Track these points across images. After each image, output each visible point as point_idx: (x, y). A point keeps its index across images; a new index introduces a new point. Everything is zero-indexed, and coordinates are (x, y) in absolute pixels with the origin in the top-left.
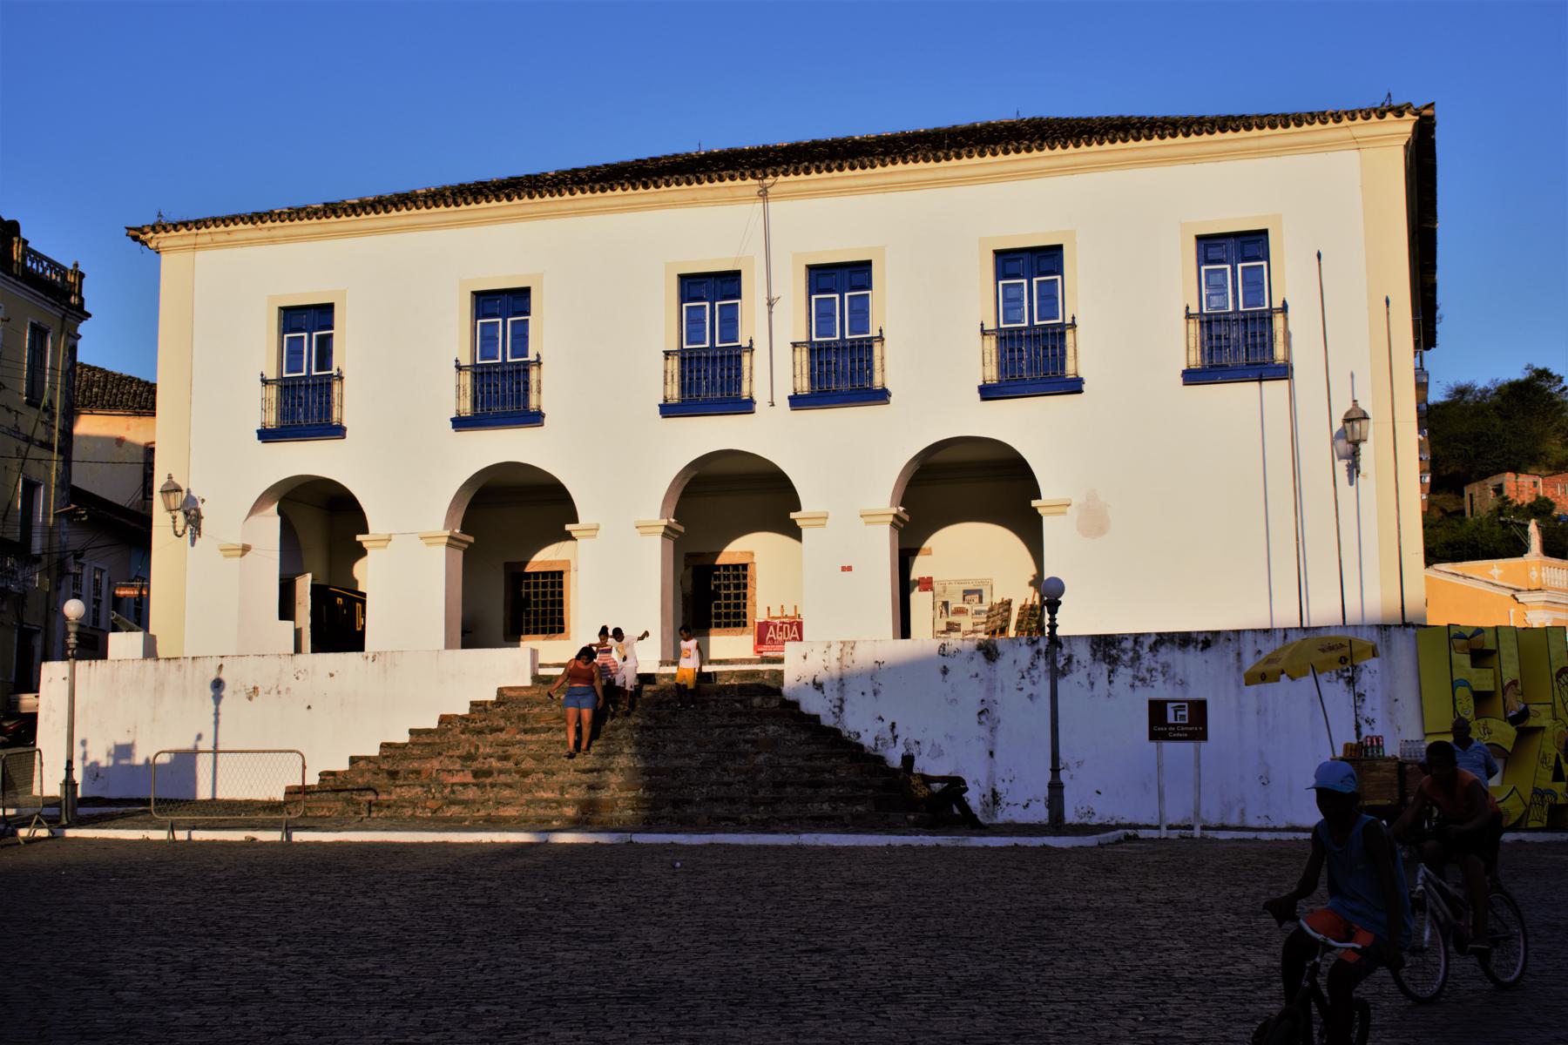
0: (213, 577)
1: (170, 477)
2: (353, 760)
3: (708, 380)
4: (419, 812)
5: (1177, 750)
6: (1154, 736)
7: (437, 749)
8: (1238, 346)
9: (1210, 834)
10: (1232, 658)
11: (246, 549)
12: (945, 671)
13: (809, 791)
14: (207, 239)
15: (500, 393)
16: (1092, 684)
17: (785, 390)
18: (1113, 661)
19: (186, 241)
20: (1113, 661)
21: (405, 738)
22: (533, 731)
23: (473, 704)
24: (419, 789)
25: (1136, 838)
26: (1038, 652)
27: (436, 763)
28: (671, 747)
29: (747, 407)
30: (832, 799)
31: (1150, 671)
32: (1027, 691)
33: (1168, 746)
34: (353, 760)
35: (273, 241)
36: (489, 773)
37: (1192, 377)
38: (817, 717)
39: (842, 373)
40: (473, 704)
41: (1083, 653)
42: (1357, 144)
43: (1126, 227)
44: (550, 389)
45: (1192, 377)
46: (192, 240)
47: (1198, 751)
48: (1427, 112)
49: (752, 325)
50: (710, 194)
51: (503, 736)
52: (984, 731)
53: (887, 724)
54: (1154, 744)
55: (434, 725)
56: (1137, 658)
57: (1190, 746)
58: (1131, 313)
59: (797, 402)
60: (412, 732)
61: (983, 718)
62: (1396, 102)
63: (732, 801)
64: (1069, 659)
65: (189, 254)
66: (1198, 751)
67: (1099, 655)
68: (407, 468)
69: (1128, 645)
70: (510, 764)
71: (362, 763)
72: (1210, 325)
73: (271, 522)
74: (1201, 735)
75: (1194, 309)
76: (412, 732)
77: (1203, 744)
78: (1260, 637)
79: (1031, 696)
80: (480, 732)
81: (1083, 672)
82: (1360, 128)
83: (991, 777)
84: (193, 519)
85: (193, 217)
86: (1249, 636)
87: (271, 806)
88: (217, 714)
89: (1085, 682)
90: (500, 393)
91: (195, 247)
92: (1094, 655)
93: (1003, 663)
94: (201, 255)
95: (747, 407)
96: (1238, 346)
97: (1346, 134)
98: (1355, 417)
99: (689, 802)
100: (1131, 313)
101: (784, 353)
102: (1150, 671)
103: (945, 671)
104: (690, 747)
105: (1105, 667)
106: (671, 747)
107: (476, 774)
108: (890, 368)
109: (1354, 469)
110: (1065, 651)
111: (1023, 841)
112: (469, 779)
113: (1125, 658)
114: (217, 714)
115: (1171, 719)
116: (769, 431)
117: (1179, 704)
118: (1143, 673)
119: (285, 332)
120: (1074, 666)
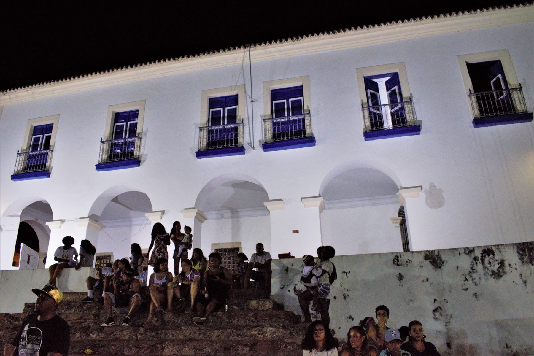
12: (401, 277)
16: (525, 282)
26: (476, 259)
32: (471, 291)
37: (478, 122)
38: (361, 321)
41: (512, 257)
59: (267, 146)
61: (437, 315)
64: (502, 263)
67: (525, 259)
79: (475, 295)
89: (520, 281)
92: (522, 259)
103: (401, 277)
110: (498, 257)
119: (33, 135)
120: (507, 268)
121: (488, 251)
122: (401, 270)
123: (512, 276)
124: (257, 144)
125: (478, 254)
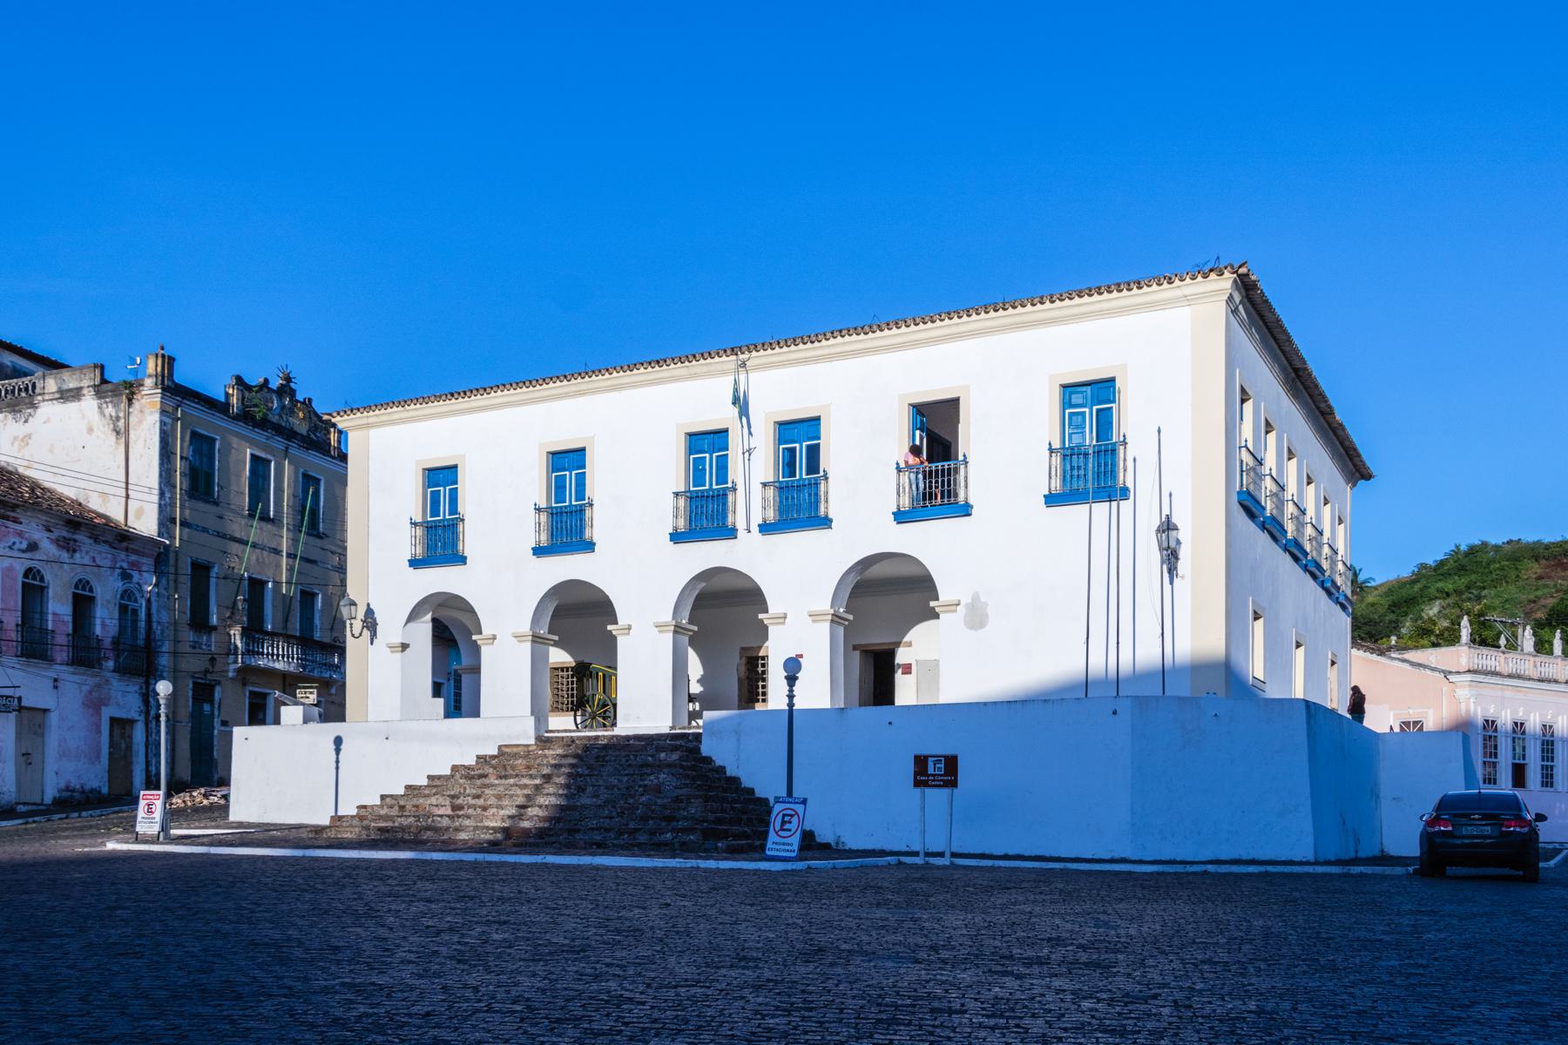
0: (386, 667)
2: (383, 797)
3: (705, 513)
5: (937, 796)
6: (917, 784)
8: (1090, 469)
9: (932, 860)
11: (404, 647)
15: (566, 527)
17: (757, 519)
21: (425, 782)
22: (506, 777)
23: (478, 757)
25: (900, 863)
27: (433, 800)
29: (731, 533)
33: (928, 790)
34: (383, 797)
36: (461, 808)
37: (1052, 500)
39: (799, 503)
40: (478, 757)
44: (600, 525)
45: (1052, 500)
48: (1243, 270)
49: (735, 473)
50: (705, 369)
51: (486, 781)
54: (918, 790)
55: (448, 772)
57: (945, 792)
58: (1009, 450)
59: (765, 528)
60: (429, 777)
68: (505, 585)
72: (1069, 455)
74: (953, 784)
75: (1056, 445)
76: (429, 777)
80: (472, 778)
84: (370, 623)
88: (337, 762)
90: (566, 527)
91: (368, 426)
95: (731, 533)
96: (1090, 469)
100: (1009, 450)
101: (757, 490)
108: (837, 498)
109: (1172, 571)
112: (449, 812)
114: (337, 762)
115: (931, 771)
116: (749, 553)
124: (755, 529)
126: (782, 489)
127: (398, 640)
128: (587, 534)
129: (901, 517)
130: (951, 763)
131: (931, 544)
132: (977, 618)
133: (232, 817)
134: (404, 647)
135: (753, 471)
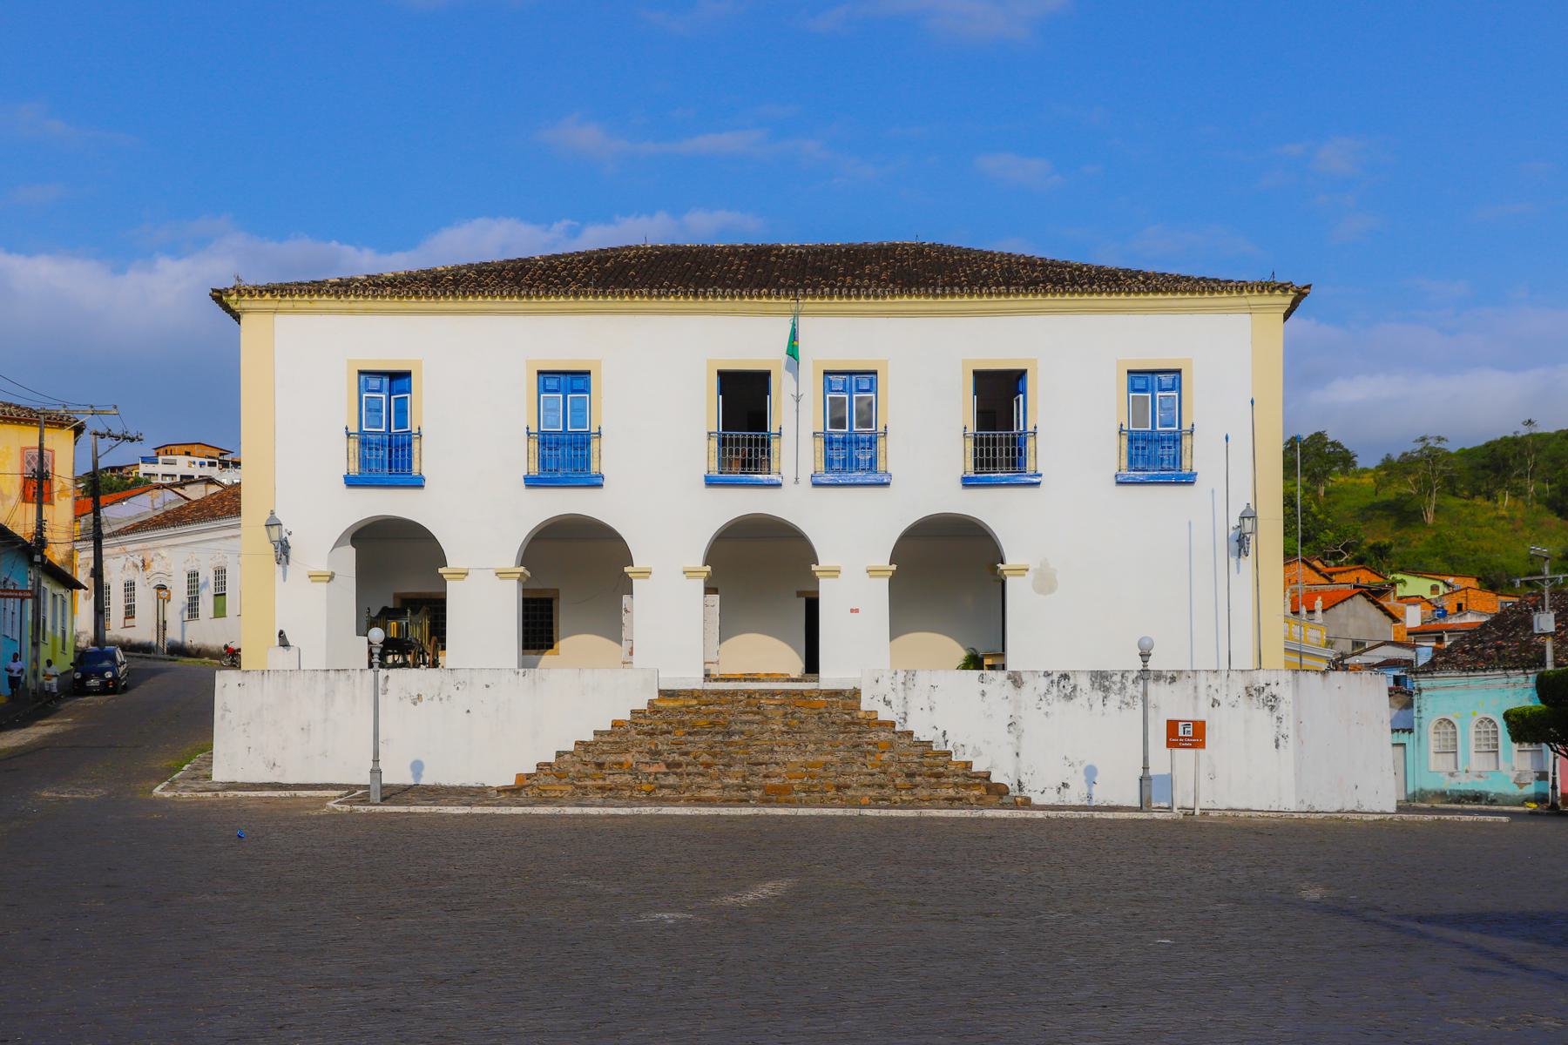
1: (272, 513)
4: (635, 793)
5: (1185, 755)
6: (1170, 745)
7: (624, 746)
8: (1155, 454)
10: (1190, 690)
12: (983, 694)
13: (933, 780)
14: (289, 305)
15: (564, 455)
18: (1106, 690)
19: (268, 305)
20: (1106, 690)
24: (628, 777)
28: (811, 747)
30: (956, 785)
31: (1133, 697)
33: (1177, 751)
35: (351, 312)
36: (679, 765)
41: (1084, 682)
42: (1250, 310)
43: (1075, 358)
46: (274, 305)
47: (1197, 756)
52: (1012, 738)
53: (940, 732)
56: (1123, 687)
57: (1192, 751)
60: (596, 733)
62: (1279, 280)
63: (881, 786)
64: (1075, 688)
65: (270, 316)
66: (1197, 756)
69: (1117, 678)
70: (690, 758)
71: (567, 757)
73: (350, 553)
74: (1201, 745)
76: (596, 733)
77: (1201, 751)
78: (1211, 676)
81: (1085, 697)
82: (1255, 299)
83: (1017, 770)
85: (263, 282)
86: (1203, 675)
87: (505, 790)
90: (564, 455)
91: (276, 311)
93: (1027, 689)
94: (279, 318)
96: (1155, 454)
97: (1244, 301)
98: (1249, 515)
99: (848, 787)
102: (1133, 697)
103: (983, 694)
104: (826, 747)
105: (1101, 694)
106: (811, 747)
107: (668, 766)
110: (1072, 681)
111: (1097, 815)
112: (664, 769)
113: (1115, 688)
115: (1181, 734)
117: (1187, 723)
118: (1128, 699)
120: (1078, 692)
121: (1065, 676)
122: (984, 687)
123: (1080, 700)
125: (1055, 677)
126: (829, 442)
127: (324, 568)
128: (594, 468)
129: (967, 483)
130: (1199, 728)
131: (994, 508)
132: (1046, 584)
133: (215, 778)
134: (332, 577)
135: (796, 418)
